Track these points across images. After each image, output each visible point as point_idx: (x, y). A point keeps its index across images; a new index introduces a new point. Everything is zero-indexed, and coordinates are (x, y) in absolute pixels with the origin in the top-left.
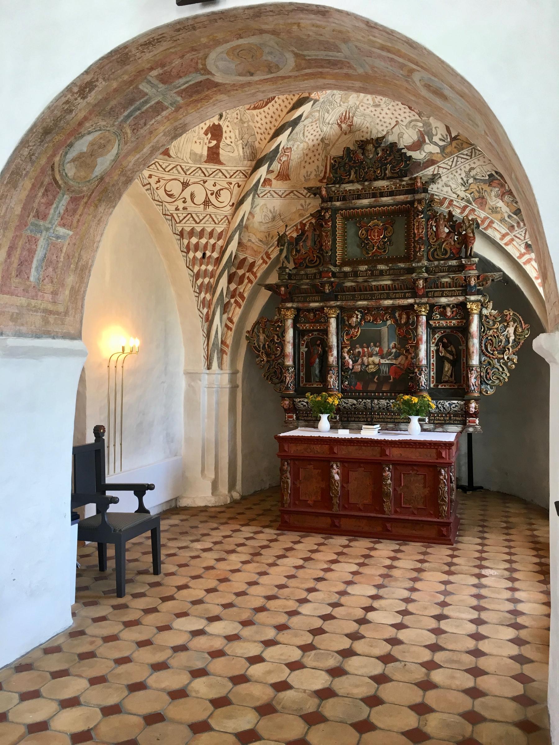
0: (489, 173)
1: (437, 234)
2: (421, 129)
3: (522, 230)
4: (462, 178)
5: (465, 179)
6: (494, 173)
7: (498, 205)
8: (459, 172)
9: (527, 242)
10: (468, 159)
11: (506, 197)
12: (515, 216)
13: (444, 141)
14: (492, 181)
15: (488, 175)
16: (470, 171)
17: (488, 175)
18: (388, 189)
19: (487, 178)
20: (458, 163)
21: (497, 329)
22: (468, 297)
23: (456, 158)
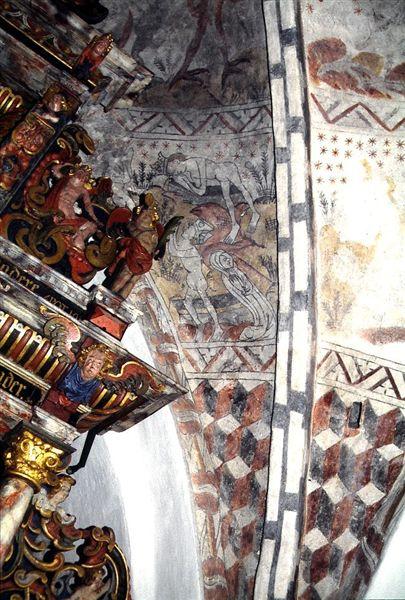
0: (213, 183)
1: (52, 195)
2: (136, 15)
3: (212, 345)
4: (142, 165)
5: (147, 170)
6: (225, 187)
7: (188, 264)
8: (146, 148)
9: (206, 380)
10: (184, 133)
11: (219, 254)
12: (211, 308)
13: (162, 69)
14: (208, 205)
15: (208, 188)
16: (171, 159)
17: (208, 188)
18: (8, 17)
19: (202, 192)
20: (159, 130)
21: (51, 575)
22: (41, 414)
23: (160, 116)
